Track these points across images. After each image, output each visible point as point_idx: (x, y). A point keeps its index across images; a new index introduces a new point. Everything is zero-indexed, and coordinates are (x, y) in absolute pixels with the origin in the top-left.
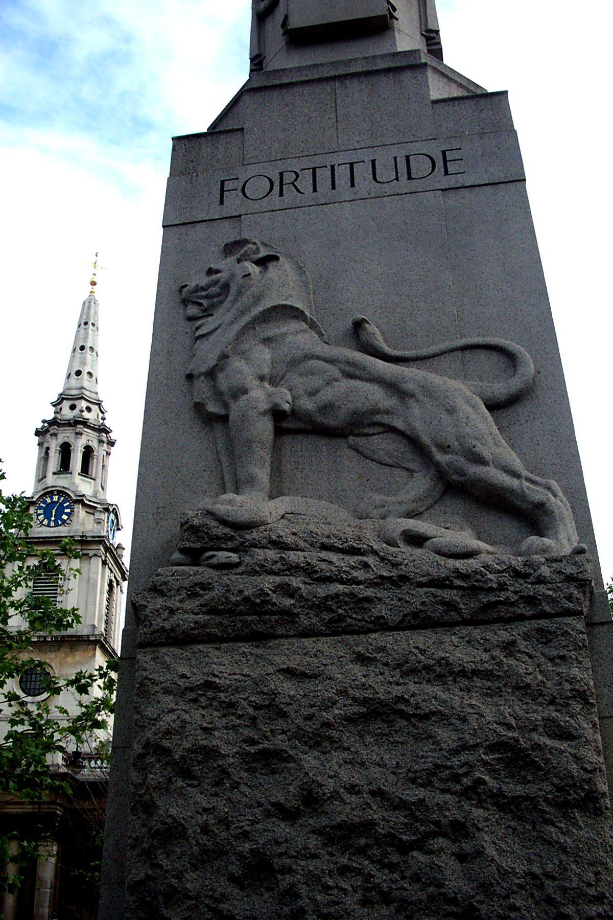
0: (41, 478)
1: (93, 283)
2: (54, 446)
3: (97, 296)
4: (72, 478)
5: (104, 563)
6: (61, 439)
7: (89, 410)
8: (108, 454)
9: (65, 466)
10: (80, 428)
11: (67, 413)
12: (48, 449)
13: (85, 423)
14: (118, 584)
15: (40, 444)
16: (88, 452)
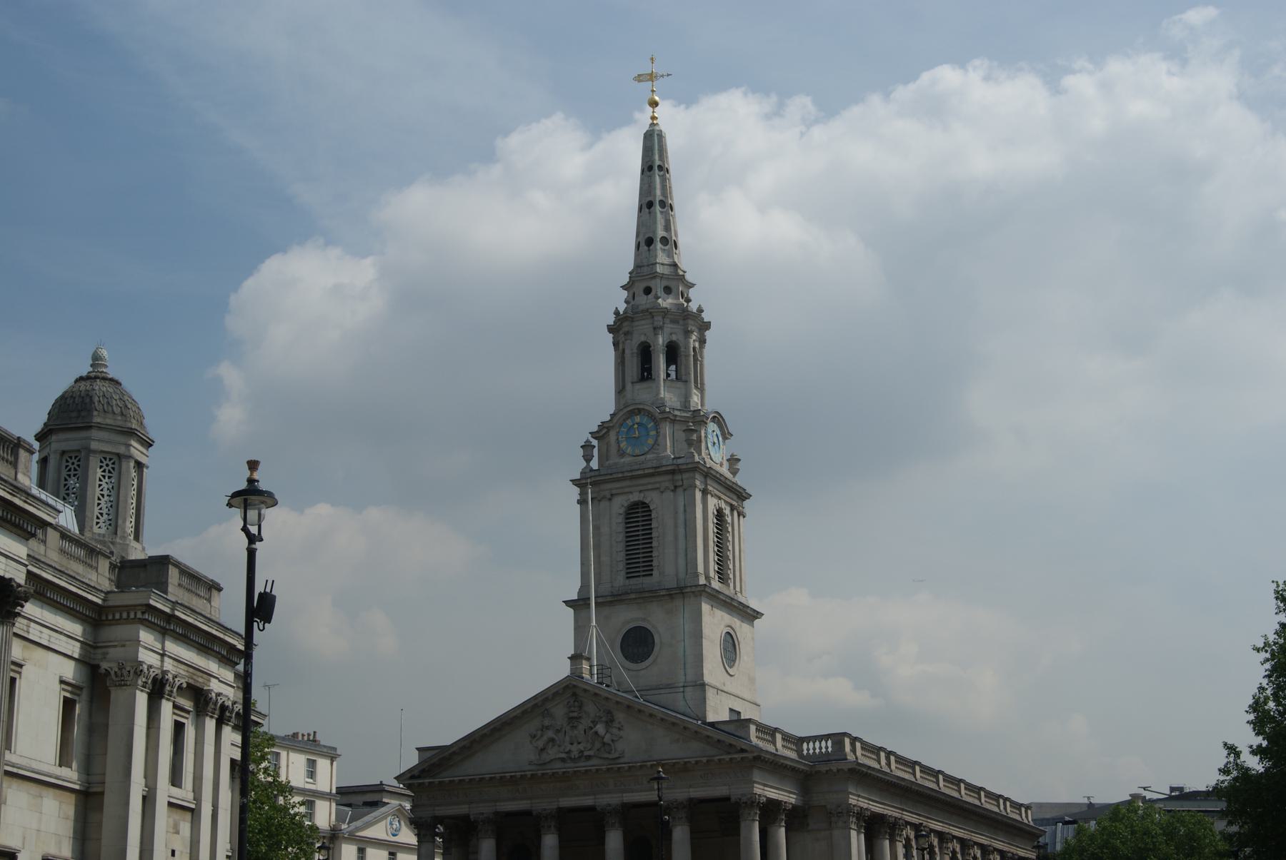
0: (620, 390)
1: (654, 104)
2: (632, 346)
3: (663, 125)
4: (658, 388)
5: (705, 492)
6: (638, 339)
7: (668, 290)
8: (702, 341)
9: (646, 373)
10: (658, 320)
11: (643, 301)
12: (624, 351)
13: (665, 312)
14: (732, 508)
15: (616, 344)
16: (673, 353)
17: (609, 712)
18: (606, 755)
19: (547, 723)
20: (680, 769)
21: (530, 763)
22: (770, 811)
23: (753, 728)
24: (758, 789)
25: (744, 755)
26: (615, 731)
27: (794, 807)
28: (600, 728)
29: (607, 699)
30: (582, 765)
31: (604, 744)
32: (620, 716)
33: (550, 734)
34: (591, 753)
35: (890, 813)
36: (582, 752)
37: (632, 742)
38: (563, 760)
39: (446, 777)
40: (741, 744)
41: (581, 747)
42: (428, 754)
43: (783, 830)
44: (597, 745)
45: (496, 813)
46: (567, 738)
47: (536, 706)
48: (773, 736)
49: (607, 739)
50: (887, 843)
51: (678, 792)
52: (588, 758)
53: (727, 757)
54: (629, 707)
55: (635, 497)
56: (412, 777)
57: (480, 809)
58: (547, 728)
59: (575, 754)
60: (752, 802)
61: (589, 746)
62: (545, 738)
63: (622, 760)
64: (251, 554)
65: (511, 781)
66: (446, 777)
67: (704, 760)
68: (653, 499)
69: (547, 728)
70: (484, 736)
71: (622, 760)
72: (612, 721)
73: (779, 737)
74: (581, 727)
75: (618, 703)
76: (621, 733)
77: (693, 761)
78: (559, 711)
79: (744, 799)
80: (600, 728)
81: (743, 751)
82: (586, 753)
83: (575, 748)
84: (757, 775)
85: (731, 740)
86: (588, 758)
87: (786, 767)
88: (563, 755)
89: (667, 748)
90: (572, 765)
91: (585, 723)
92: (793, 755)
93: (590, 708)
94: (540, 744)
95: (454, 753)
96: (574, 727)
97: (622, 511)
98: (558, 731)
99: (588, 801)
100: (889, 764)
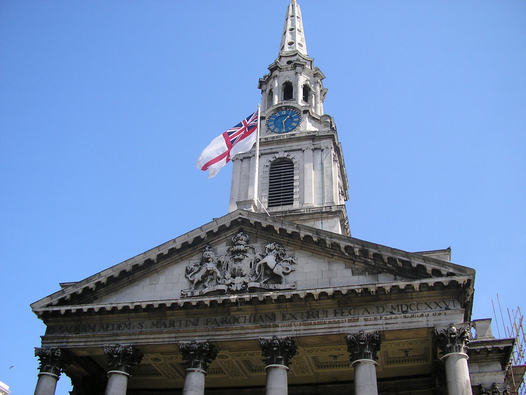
25: (455, 278)
28: (270, 260)
33: (211, 266)
34: (257, 285)
36: (245, 283)
37: (308, 274)
38: (221, 292)
49: (278, 270)
52: (253, 290)
55: (281, 155)
56: (50, 305)
68: (296, 157)
69: (207, 260)
72: (284, 255)
82: (251, 285)
83: (238, 280)
91: (250, 257)
94: (198, 277)
97: (269, 164)
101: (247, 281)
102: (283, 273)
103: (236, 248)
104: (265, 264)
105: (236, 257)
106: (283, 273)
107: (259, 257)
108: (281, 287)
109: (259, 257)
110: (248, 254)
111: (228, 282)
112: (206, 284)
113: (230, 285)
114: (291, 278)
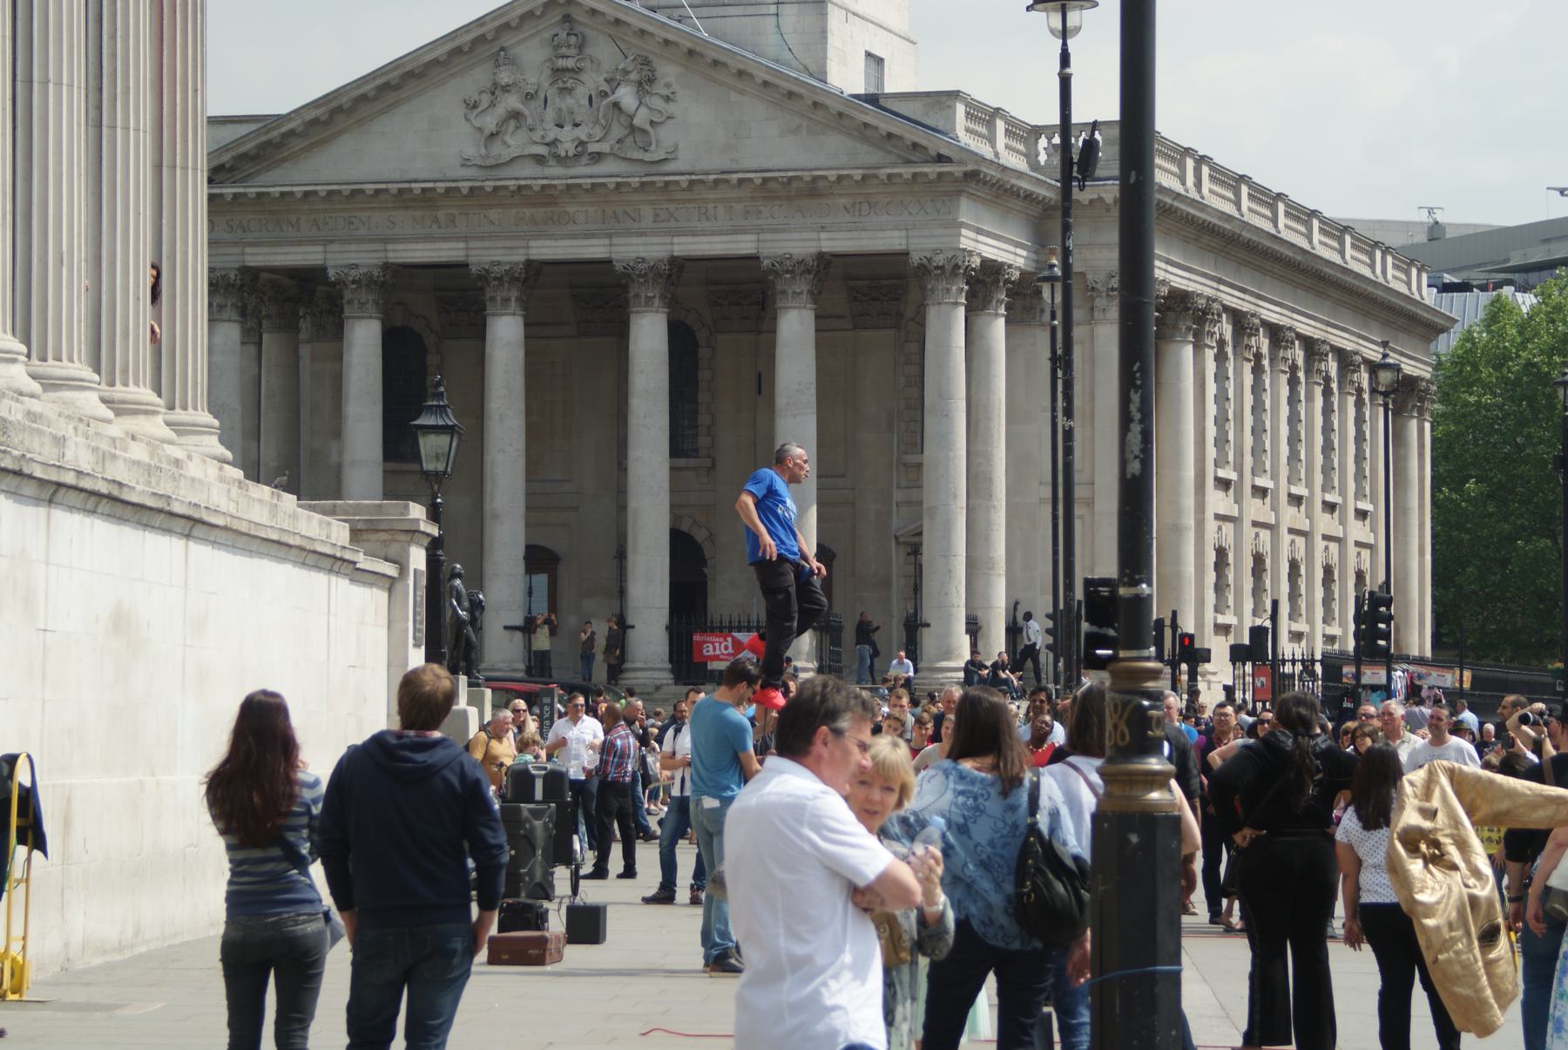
17: (646, 62)
18: (640, 155)
19: (505, 77)
20: (804, 191)
21: (466, 163)
22: (984, 282)
23: (960, 109)
24: (967, 240)
26: (656, 102)
27: (1023, 273)
28: (626, 96)
29: (643, 32)
30: (583, 172)
31: (633, 129)
32: (668, 72)
33: (512, 102)
34: (604, 147)
35: (1199, 288)
36: (582, 143)
37: (697, 131)
38: (539, 159)
39: (274, 181)
40: (935, 144)
41: (582, 133)
42: (229, 134)
43: (1000, 323)
44: (617, 131)
45: (386, 266)
46: (550, 114)
47: (481, 39)
48: (990, 124)
50: (1188, 350)
51: (796, 239)
52: (597, 157)
53: (906, 171)
54: (691, 52)
57: (348, 257)
58: (506, 89)
59: (567, 147)
60: (953, 268)
61: (598, 132)
62: (501, 110)
63: (671, 167)
64: (1065, 59)
65: (421, 200)
66: (274, 181)
67: (857, 174)
69: (506, 89)
70: (363, 98)
71: (671, 167)
72: (651, 81)
73: (1000, 126)
74: (582, 93)
75: (667, 42)
76: (672, 108)
77: (832, 175)
78: (532, 56)
79: (940, 260)
80: (626, 96)
81: (940, 159)
82: (592, 148)
83: (567, 136)
84: (966, 211)
85: (912, 134)
86: (597, 157)
87: (1014, 192)
88: (542, 150)
89: (776, 147)
90: (558, 171)
91: (592, 81)
92: (1018, 163)
93: (604, 52)
94: (490, 122)
95: (292, 133)
96: (566, 91)
98: (529, 97)
99: (594, 249)
100: (1198, 185)
101: (584, 138)
102: (652, 123)
103: (561, 63)
104: (616, 105)
105: (561, 85)
106: (652, 123)
107: (605, 87)
108: (647, 157)
109: (605, 87)
110: (584, 77)
111: (550, 137)
112: (508, 138)
113: (554, 143)
114: (666, 136)
